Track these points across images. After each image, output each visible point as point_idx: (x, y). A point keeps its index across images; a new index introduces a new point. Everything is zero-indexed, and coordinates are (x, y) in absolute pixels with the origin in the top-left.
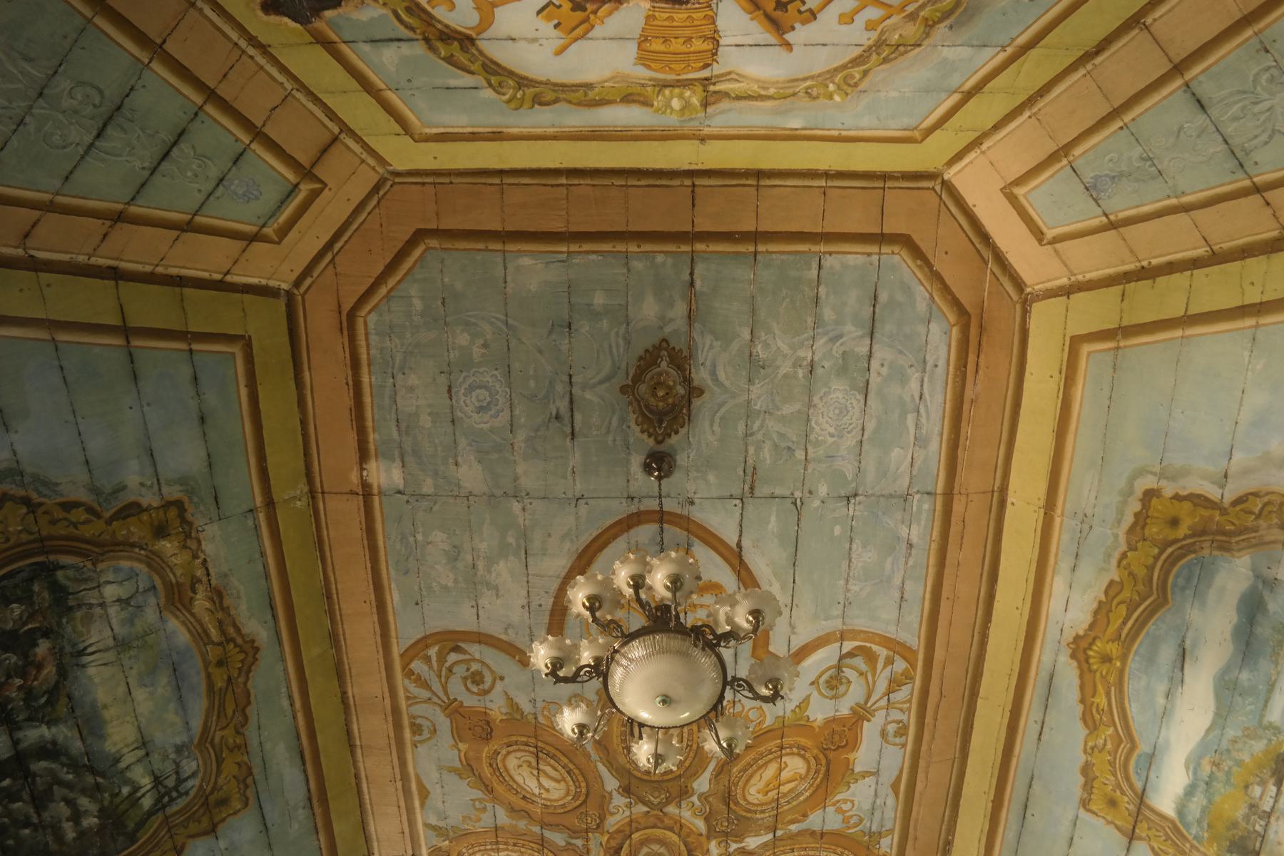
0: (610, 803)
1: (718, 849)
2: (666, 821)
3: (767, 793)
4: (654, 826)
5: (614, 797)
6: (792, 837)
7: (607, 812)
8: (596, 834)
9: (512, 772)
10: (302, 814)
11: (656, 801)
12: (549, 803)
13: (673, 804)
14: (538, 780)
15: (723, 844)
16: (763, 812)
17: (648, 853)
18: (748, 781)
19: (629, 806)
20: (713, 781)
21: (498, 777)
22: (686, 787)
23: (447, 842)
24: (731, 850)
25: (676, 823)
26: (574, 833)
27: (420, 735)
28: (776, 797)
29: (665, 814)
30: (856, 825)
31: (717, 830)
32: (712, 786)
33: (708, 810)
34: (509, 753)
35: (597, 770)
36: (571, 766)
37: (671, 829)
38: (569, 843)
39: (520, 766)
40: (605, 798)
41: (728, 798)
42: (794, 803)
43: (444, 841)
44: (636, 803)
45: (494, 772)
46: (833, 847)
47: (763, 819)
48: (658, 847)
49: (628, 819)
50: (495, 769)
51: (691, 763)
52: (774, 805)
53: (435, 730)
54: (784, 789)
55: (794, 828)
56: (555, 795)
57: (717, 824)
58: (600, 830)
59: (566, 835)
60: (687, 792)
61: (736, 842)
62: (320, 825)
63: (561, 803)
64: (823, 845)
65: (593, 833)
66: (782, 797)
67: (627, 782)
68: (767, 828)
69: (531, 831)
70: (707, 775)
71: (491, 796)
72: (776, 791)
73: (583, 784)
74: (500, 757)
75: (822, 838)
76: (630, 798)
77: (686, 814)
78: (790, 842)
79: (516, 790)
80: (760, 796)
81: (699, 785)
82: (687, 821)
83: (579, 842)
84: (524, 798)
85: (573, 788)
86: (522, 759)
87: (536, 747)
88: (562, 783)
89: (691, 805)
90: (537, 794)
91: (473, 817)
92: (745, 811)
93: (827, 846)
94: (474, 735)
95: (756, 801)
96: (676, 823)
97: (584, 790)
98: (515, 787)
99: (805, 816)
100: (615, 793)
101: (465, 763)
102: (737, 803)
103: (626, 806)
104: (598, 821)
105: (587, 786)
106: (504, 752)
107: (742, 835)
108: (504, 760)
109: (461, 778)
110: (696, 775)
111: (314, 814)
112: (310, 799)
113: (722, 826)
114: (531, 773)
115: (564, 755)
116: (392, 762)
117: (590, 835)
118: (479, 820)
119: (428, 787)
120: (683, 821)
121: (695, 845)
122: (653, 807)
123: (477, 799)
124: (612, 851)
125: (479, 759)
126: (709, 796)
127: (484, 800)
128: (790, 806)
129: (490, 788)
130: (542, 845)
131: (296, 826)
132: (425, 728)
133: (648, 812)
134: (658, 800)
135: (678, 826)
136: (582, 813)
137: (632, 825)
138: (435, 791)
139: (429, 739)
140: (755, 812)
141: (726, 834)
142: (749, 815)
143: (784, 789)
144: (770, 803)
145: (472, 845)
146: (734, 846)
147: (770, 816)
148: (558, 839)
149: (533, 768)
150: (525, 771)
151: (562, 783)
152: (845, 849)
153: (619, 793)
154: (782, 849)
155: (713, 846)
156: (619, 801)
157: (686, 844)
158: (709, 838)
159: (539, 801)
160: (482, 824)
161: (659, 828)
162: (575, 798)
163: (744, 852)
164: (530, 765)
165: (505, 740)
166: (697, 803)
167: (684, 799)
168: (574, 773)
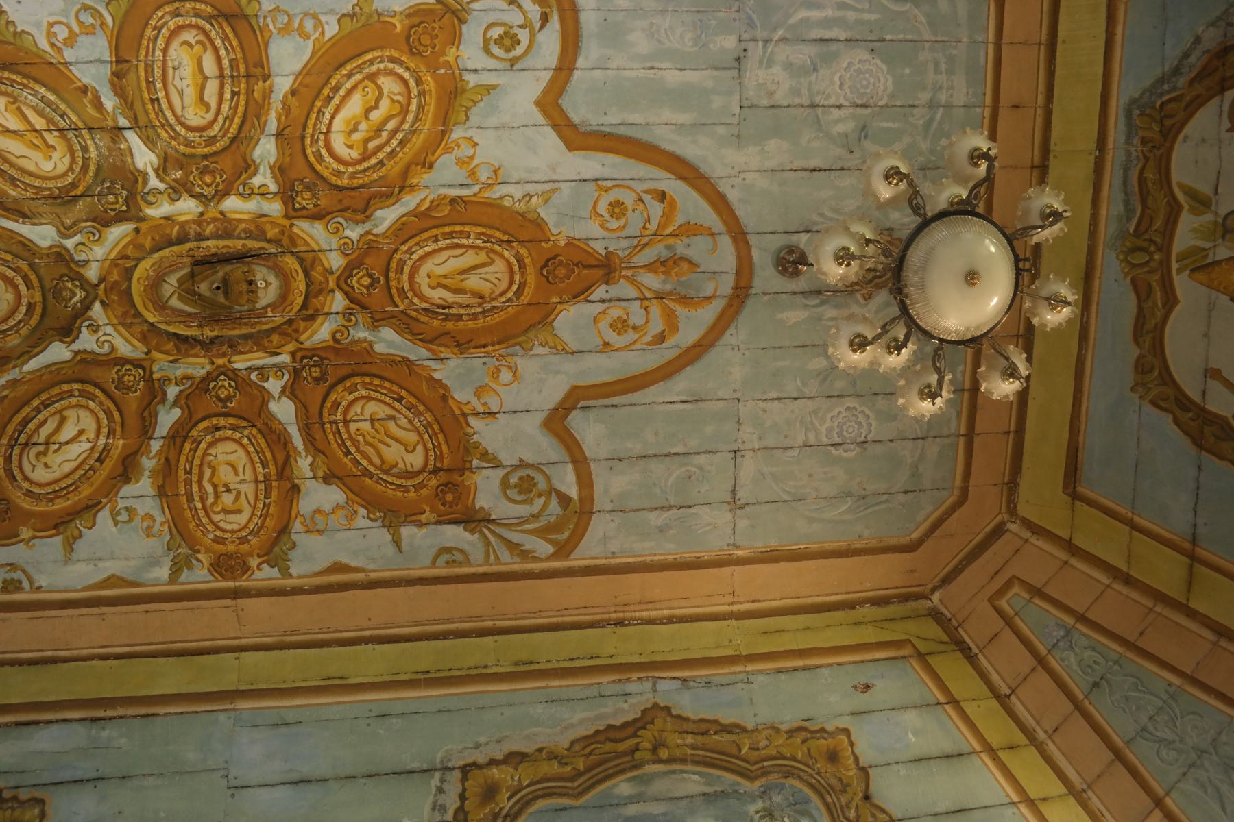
0: (93, 352)
1: (161, 205)
2: (115, 277)
3: (53, 147)
4: (128, 293)
5: (81, 348)
6: (127, 103)
7: (112, 356)
8: (155, 368)
9: (57, 475)
10: (107, 733)
11: (80, 294)
12: (106, 430)
13: (82, 271)
14: (67, 443)
15: (150, 198)
16: (85, 149)
17: (180, 298)
18: (31, 174)
19: (94, 328)
20: (36, 221)
21: (69, 493)
22: (48, 255)
23: (200, 556)
24: (162, 186)
25: (117, 265)
26: (154, 393)
27: (20, 582)
28: (56, 133)
29: (102, 280)
30: (97, 14)
31: (124, 208)
32: (44, 221)
33: (89, 224)
34: (26, 478)
35: (39, 370)
36: (36, 403)
37: (128, 273)
38: (176, 403)
39: (46, 465)
40: (86, 360)
41: (65, 197)
42: (63, 107)
43: (199, 560)
44: (90, 318)
45: (60, 497)
46: (145, 43)
47: (97, 148)
48: (166, 286)
49: (120, 328)
50: (56, 495)
51: (6, 252)
52: (70, 135)
53: (11, 565)
54: (40, 123)
55: (109, 102)
56: (88, 422)
57: (111, 210)
58: (145, 364)
59: (160, 407)
60: (58, 254)
61: (145, 181)
62: (144, 711)
63: (102, 415)
64: (142, 57)
65: (152, 373)
66: (55, 124)
67: (51, 332)
68: (114, 141)
69: (159, 453)
70: (24, 229)
71: (104, 501)
72: (45, 134)
73: (66, 387)
74: (36, 490)
75: (127, 61)
76: (81, 326)
77: (99, 252)
78: (138, 106)
79: (85, 471)
80: (56, 156)
81: (44, 239)
82: (111, 251)
83: (172, 391)
84: (100, 460)
85: (74, 401)
86: (34, 461)
87: (12, 447)
88: (65, 413)
89: (81, 247)
90: (89, 445)
91: (145, 524)
92: (85, 177)
93: (143, 52)
94: (4, 520)
95: (67, 160)
96: (117, 265)
97: (76, 386)
98: (83, 472)
99: (84, 90)
100: (75, 347)
101: (54, 531)
102: (73, 185)
103: (96, 331)
104: (128, 367)
105: (70, 382)
106: (26, 485)
107: (132, 173)
108: (40, 485)
109: (80, 536)
110: (26, 247)
111: (121, 717)
112: (95, 720)
113: (117, 202)
114: (55, 451)
115: (17, 411)
116: (72, 616)
117: (155, 376)
118: (152, 518)
119: (105, 576)
120: (112, 256)
121: (157, 238)
122: (91, 297)
123: (114, 519)
124: (183, 347)
125: (43, 516)
126: (63, 224)
127: (111, 511)
128: (69, 112)
129: (90, 503)
130: (186, 438)
131: (123, 741)
132: (8, 576)
133: (102, 303)
134: (77, 291)
135: (124, 265)
136: (116, 388)
137: (129, 318)
138: (110, 568)
139: (24, 571)
140: (86, 160)
141: (131, 198)
142: (92, 168)
143: (40, 123)
144: (68, 141)
145: (198, 526)
146: (154, 182)
147: (93, 139)
148: (168, 418)
149: (47, 450)
150: (54, 459)
151: (65, 413)
152: (147, 24)
153: (74, 341)
154: (153, 116)
155: (157, 211)
156: (86, 341)
157: (157, 248)
158: (143, 219)
159: (102, 441)
160: (156, 513)
161: (129, 287)
162: (92, 397)
163: (165, 169)
164: (45, 453)
165: (7, 483)
166: (78, 238)
167: (71, 256)
168: (48, 399)
